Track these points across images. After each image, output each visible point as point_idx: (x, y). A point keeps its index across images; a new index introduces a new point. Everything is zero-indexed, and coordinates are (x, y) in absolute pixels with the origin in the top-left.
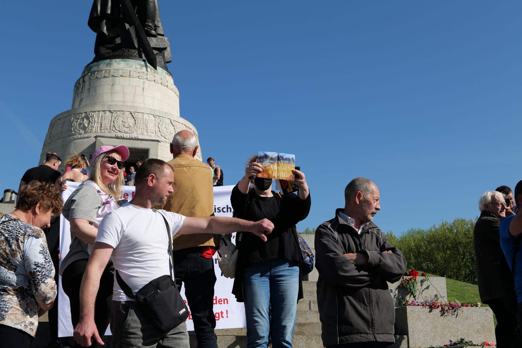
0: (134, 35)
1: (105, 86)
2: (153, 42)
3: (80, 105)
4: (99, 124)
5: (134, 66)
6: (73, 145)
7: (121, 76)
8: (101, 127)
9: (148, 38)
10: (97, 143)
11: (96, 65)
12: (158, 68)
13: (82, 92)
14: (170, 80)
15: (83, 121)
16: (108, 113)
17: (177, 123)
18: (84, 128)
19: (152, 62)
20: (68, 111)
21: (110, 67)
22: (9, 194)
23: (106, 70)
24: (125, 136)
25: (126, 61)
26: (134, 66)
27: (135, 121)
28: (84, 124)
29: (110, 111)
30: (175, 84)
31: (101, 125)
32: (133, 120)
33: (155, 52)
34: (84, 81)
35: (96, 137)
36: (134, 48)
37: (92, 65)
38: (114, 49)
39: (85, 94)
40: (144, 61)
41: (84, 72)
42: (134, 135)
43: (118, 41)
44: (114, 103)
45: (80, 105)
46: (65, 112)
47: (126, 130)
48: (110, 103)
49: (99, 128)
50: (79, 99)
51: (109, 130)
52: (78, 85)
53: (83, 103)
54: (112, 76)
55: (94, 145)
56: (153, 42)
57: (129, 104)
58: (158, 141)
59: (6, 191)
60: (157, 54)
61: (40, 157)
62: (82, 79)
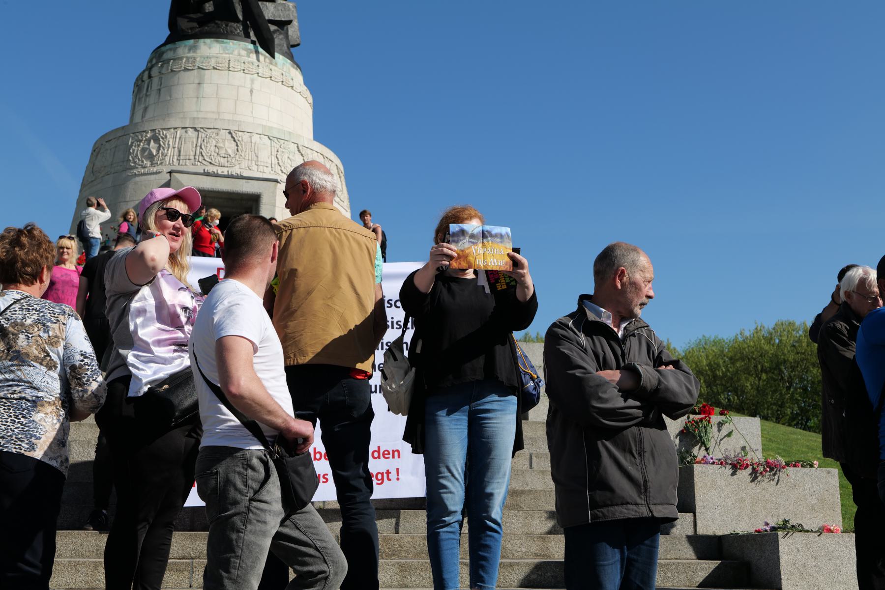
1: (186, 84)
3: (143, 117)
4: (176, 149)
5: (236, 52)
6: (131, 185)
7: (214, 68)
8: (179, 155)
9: (260, 3)
10: (172, 182)
11: (171, 49)
12: (277, 55)
13: (146, 95)
14: (297, 77)
15: (149, 144)
16: (190, 131)
17: (309, 151)
18: (151, 157)
19: (267, 45)
20: (123, 127)
21: (194, 52)
23: (188, 58)
24: (220, 172)
26: (236, 52)
27: (237, 145)
28: (150, 150)
29: (195, 129)
30: (305, 84)
31: (180, 152)
32: (234, 144)
33: (273, 28)
34: (150, 77)
35: (170, 173)
36: (237, 20)
37: (163, 49)
38: (202, 23)
39: (152, 99)
40: (253, 42)
41: (150, 61)
42: (235, 171)
43: (209, 7)
44: (201, 115)
45: (143, 117)
46: (117, 129)
47: (222, 160)
48: (195, 115)
49: (176, 157)
50: (143, 106)
51: (193, 161)
52: (140, 82)
53: (149, 114)
54: (199, 68)
56: (269, 11)
57: (227, 117)
60: (275, 31)
61: (75, 206)
62: (147, 73)
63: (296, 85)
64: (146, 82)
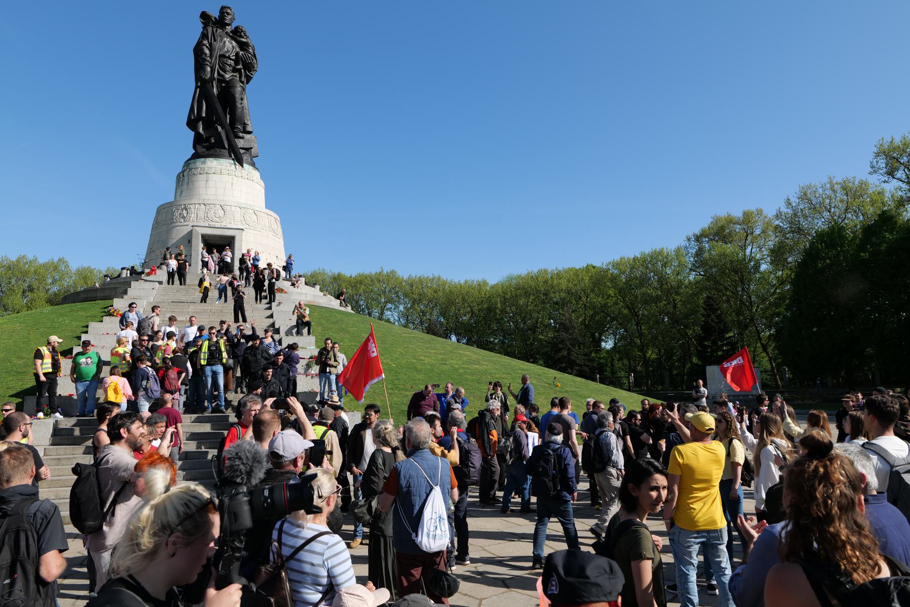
0: (224, 138)
1: (200, 181)
2: (240, 143)
6: (174, 231)
14: (256, 174)
18: (184, 217)
19: (239, 160)
22: (125, 271)
33: (242, 151)
36: (225, 148)
38: (208, 149)
39: (185, 187)
42: (223, 225)
53: (184, 194)
55: (191, 232)
56: (240, 143)
59: (123, 269)
63: (254, 179)
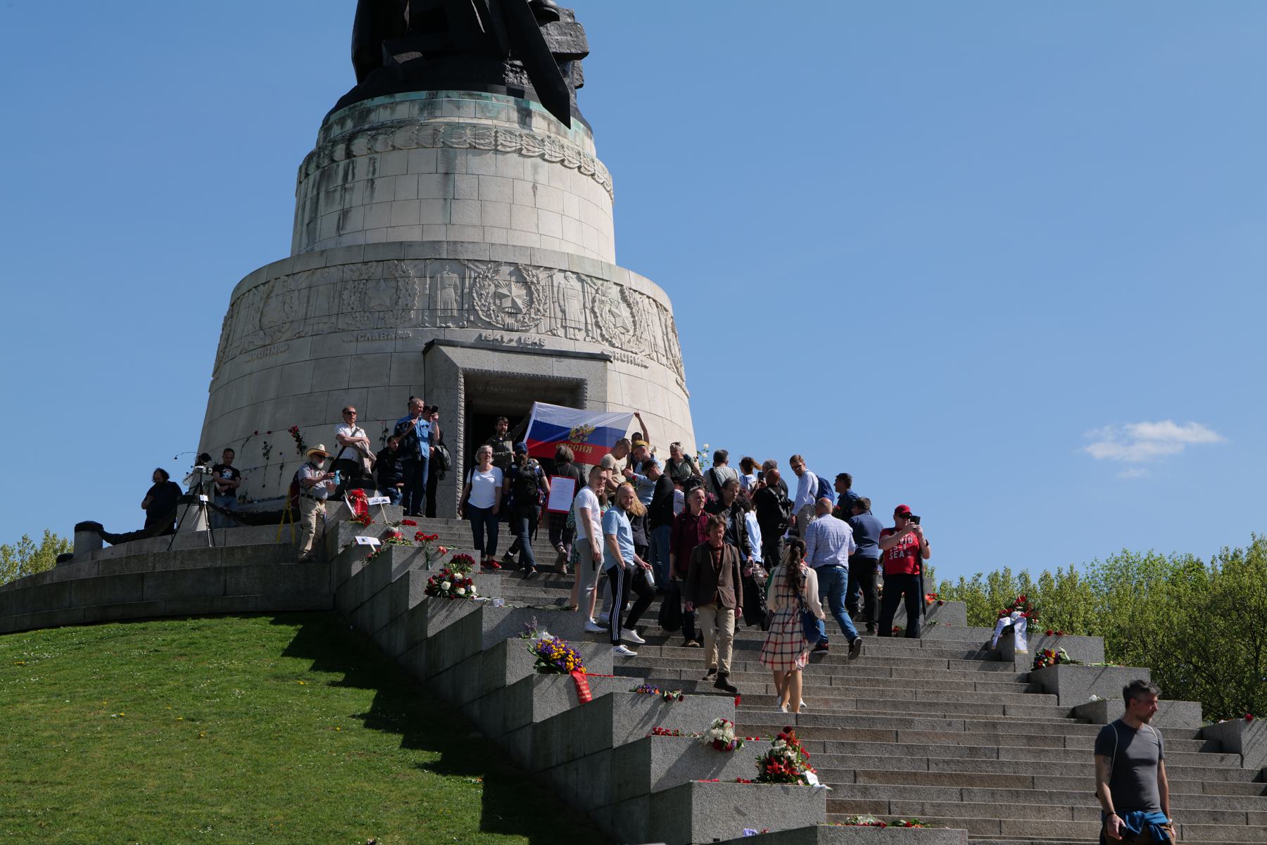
5: (503, 115)
11: (385, 106)
13: (344, 189)
17: (637, 296)
25: (480, 97)
34: (349, 154)
39: (357, 196)
42: (532, 337)
47: (509, 321)
50: (337, 207)
57: (498, 237)
58: (604, 358)
64: (342, 164)
